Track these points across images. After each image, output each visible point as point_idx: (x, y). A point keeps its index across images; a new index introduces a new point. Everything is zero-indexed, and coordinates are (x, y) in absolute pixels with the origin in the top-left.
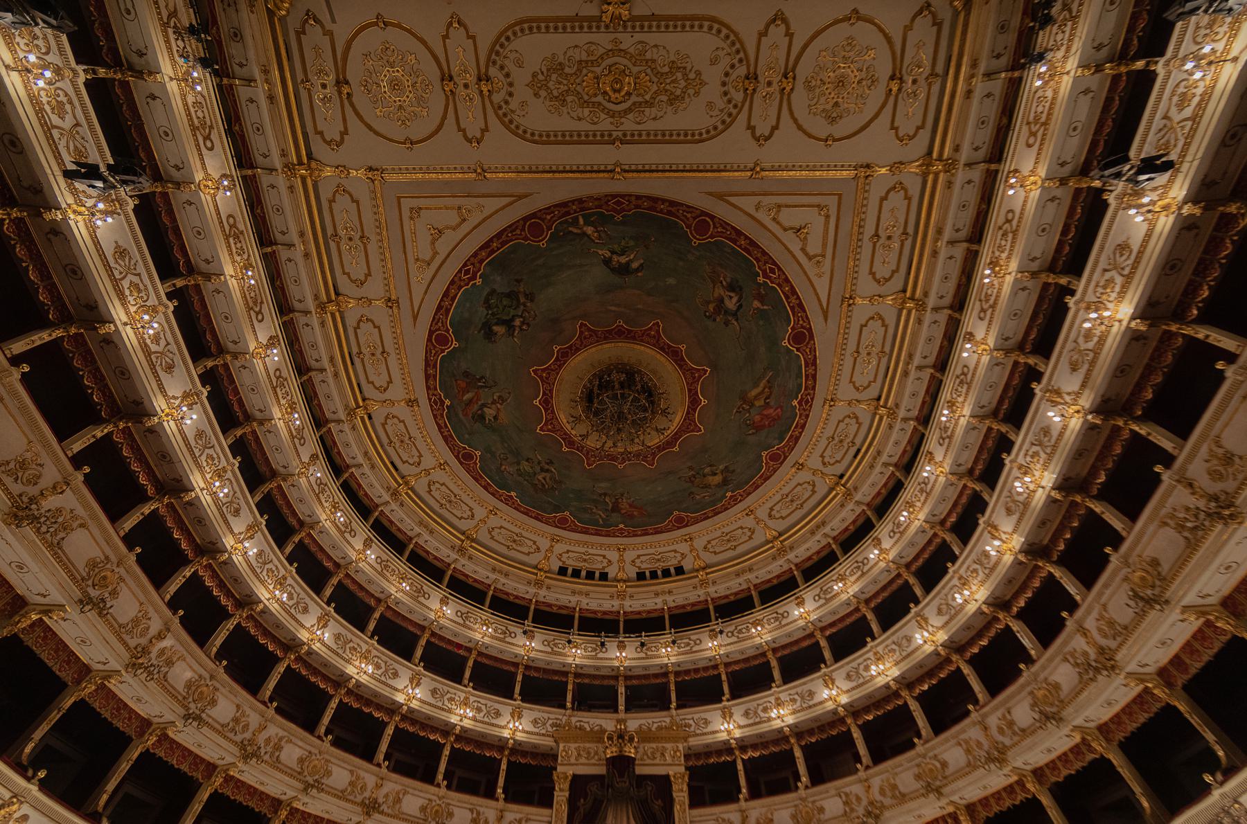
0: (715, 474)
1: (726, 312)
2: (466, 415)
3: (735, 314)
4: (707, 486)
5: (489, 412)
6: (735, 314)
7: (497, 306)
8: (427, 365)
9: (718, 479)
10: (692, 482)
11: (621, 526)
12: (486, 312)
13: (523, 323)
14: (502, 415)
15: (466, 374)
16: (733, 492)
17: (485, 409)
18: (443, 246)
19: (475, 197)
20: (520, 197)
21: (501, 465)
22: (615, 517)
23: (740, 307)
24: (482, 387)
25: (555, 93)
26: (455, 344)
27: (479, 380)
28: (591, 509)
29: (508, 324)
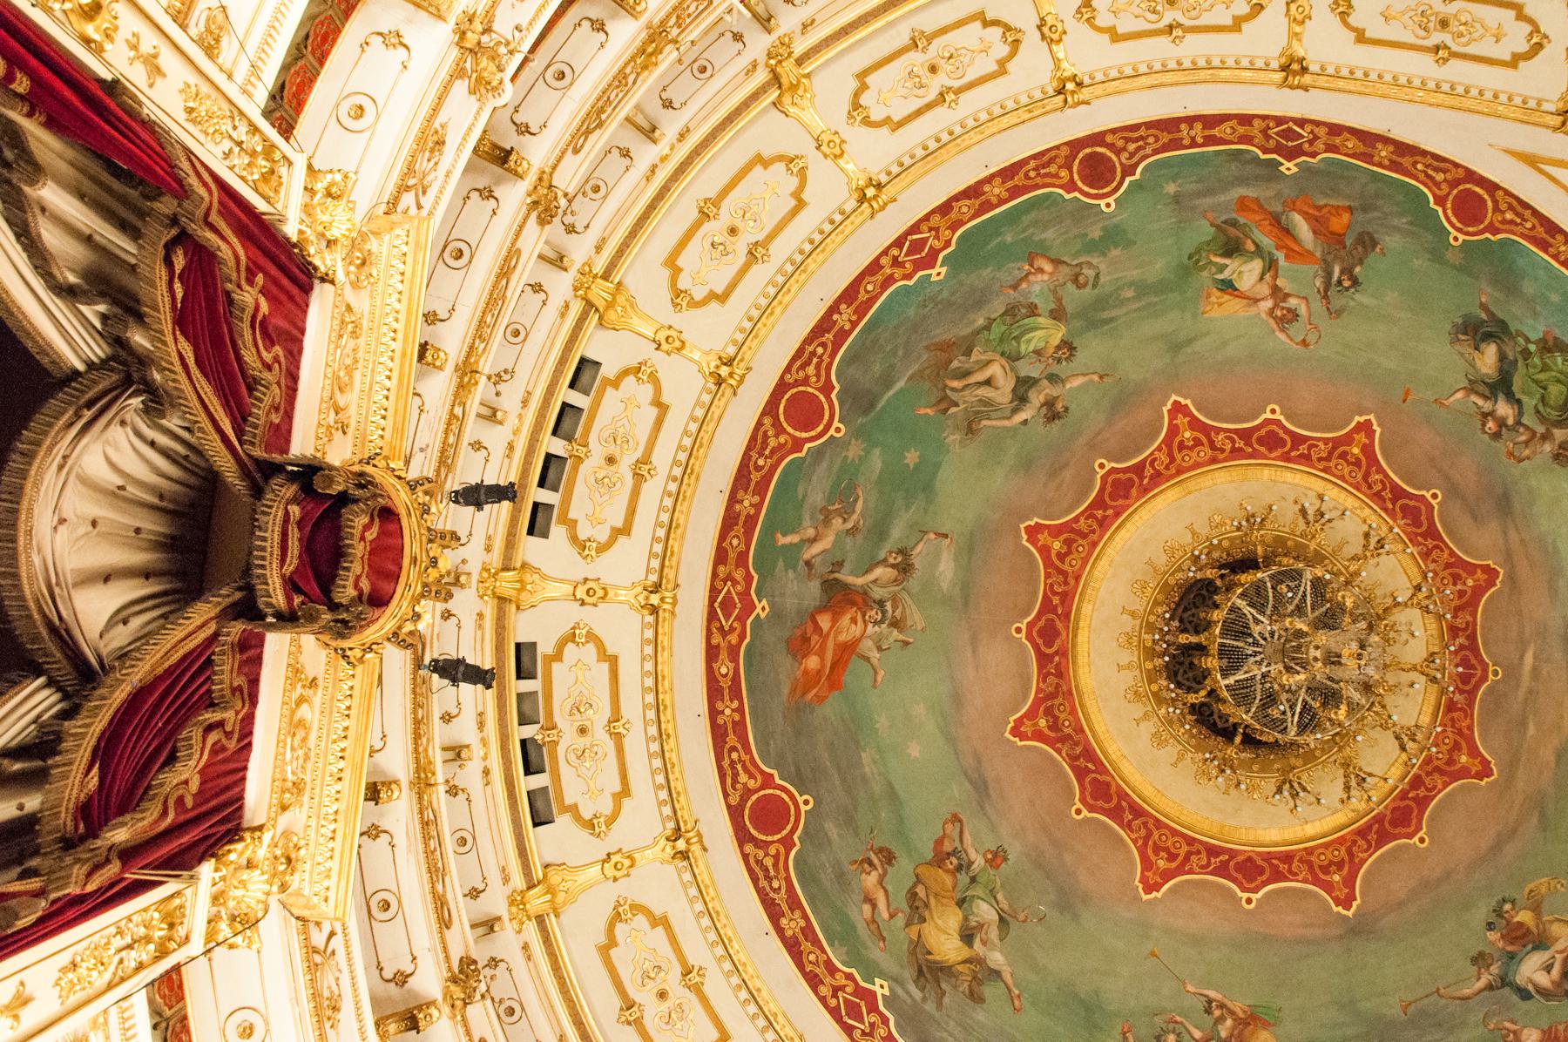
0: (967, 937)
1: (1512, 956)
2: (1243, 204)
3: (1504, 981)
4: (917, 909)
5: (1247, 273)
6: (1504, 981)
7: (1545, 368)
8: (1403, 149)
9: (946, 944)
10: (939, 859)
11: (762, 608)
12: (1533, 336)
13: (1501, 423)
14: (1233, 305)
15: (1368, 242)
16: (890, 1001)
17: (1257, 265)
21: (1057, 262)
22: (803, 592)
23: (1525, 995)
24: (1329, 274)
26: (1456, 237)
27: (1348, 271)
28: (845, 514)
29: (1501, 386)
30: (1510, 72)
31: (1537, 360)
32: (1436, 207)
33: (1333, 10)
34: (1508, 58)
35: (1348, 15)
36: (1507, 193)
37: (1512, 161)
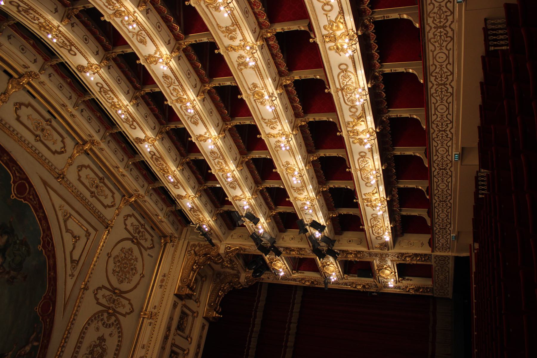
18: (68, 237)
19: (78, 276)
20: (65, 306)
25: (95, 349)
30: (52, 155)
31: (17, 246)
32: (12, 183)
33: (14, 105)
34: (54, 150)
35: (18, 110)
36: (34, 190)
37: (40, 180)
